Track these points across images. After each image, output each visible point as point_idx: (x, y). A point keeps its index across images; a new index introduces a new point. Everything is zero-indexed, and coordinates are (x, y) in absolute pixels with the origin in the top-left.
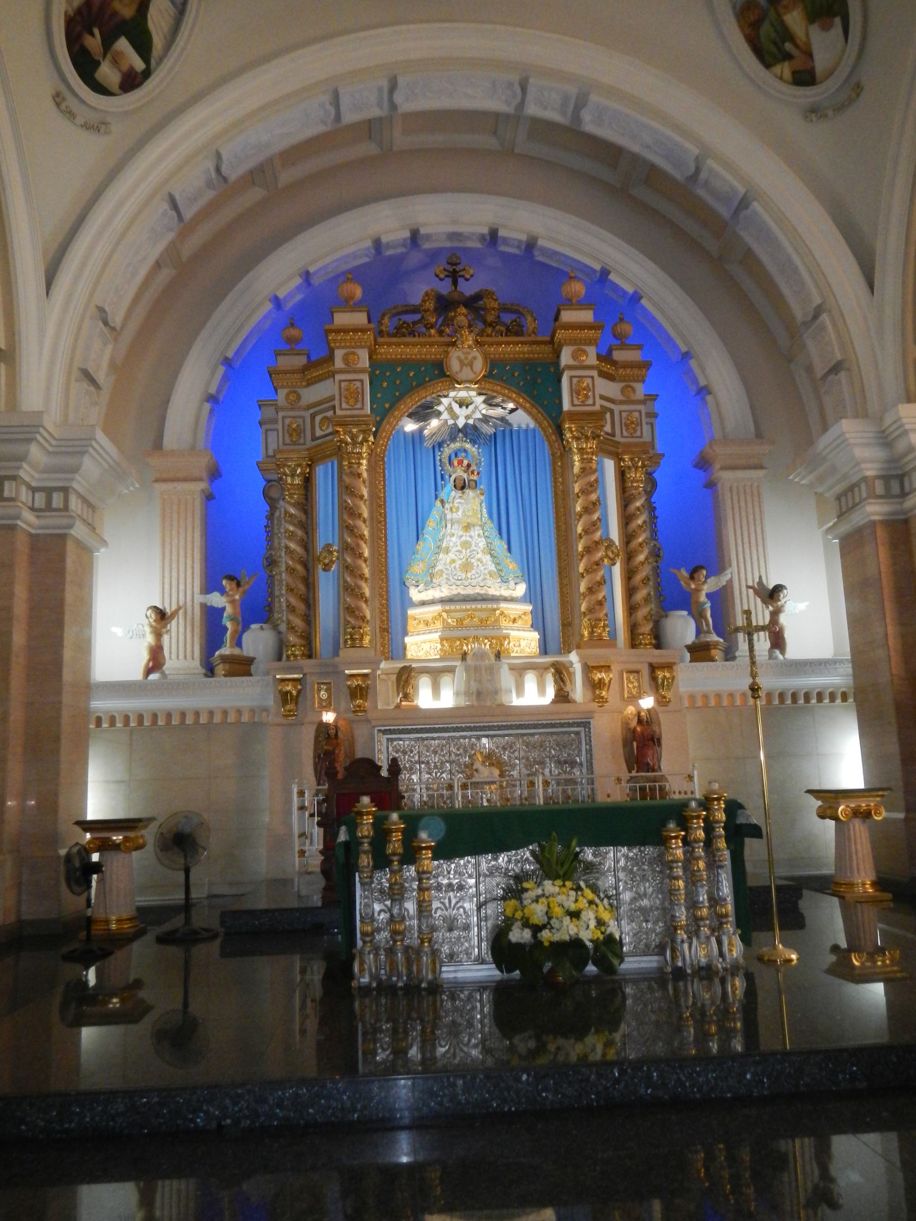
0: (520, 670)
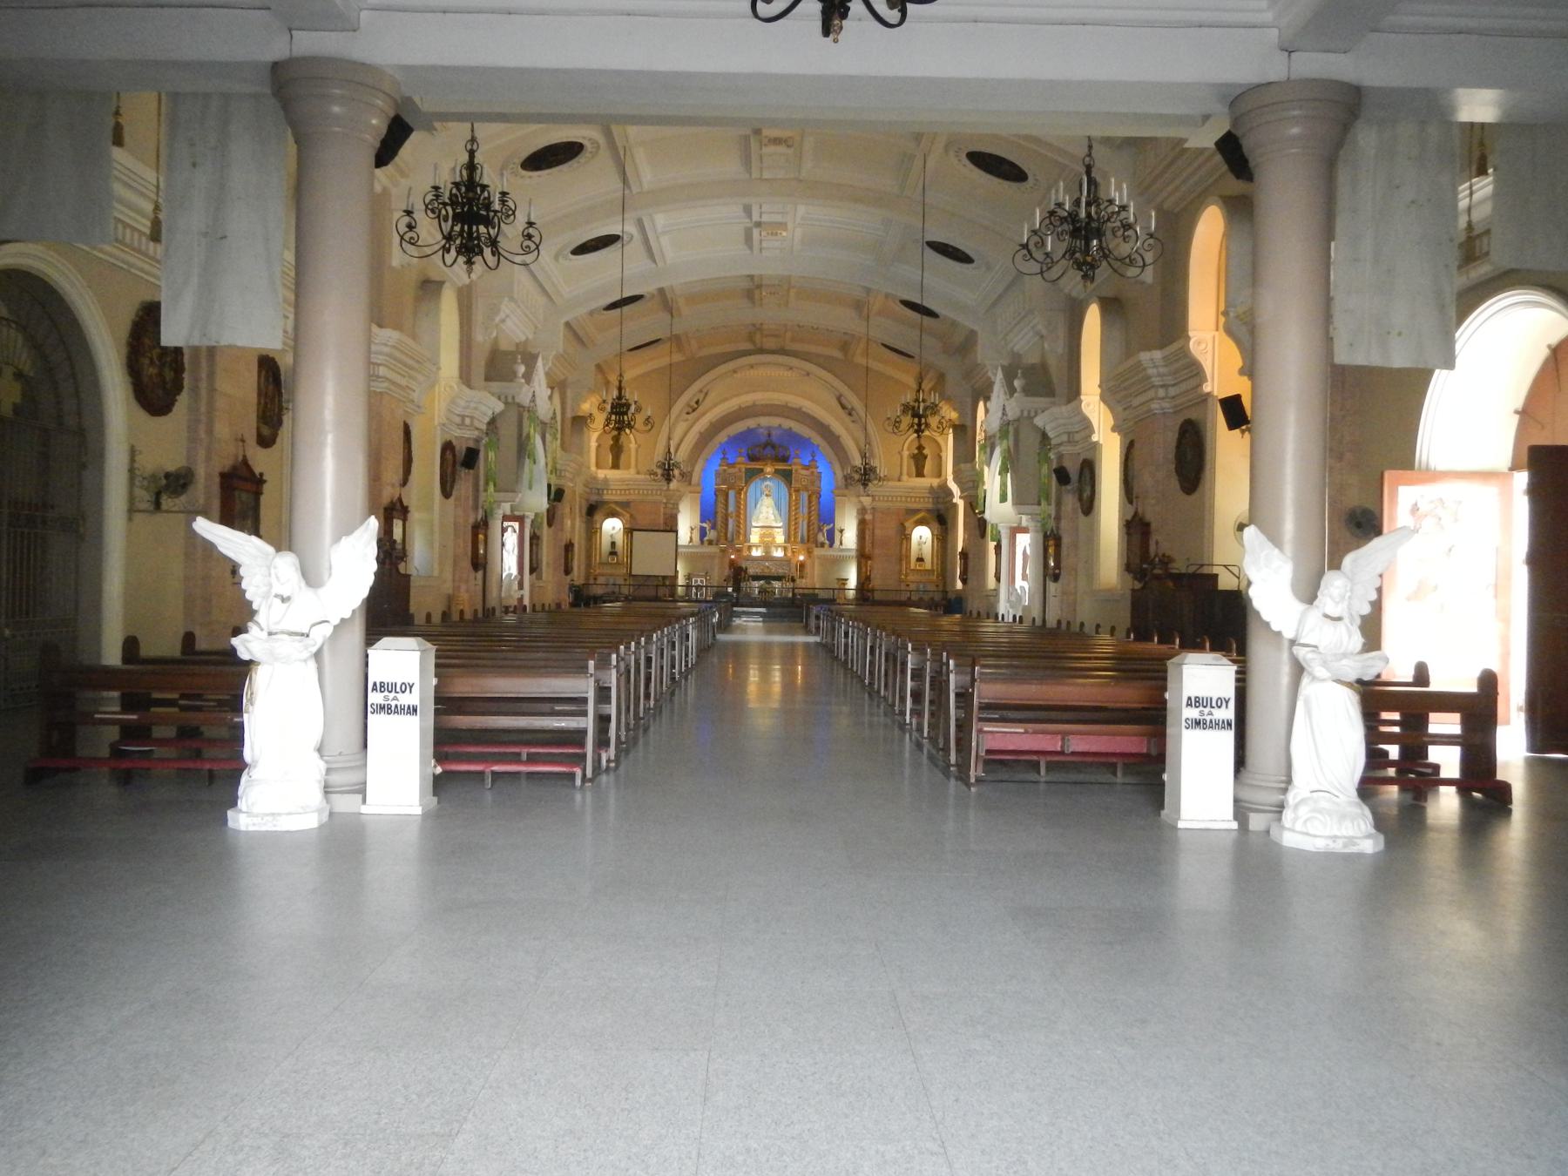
0: (777, 547)
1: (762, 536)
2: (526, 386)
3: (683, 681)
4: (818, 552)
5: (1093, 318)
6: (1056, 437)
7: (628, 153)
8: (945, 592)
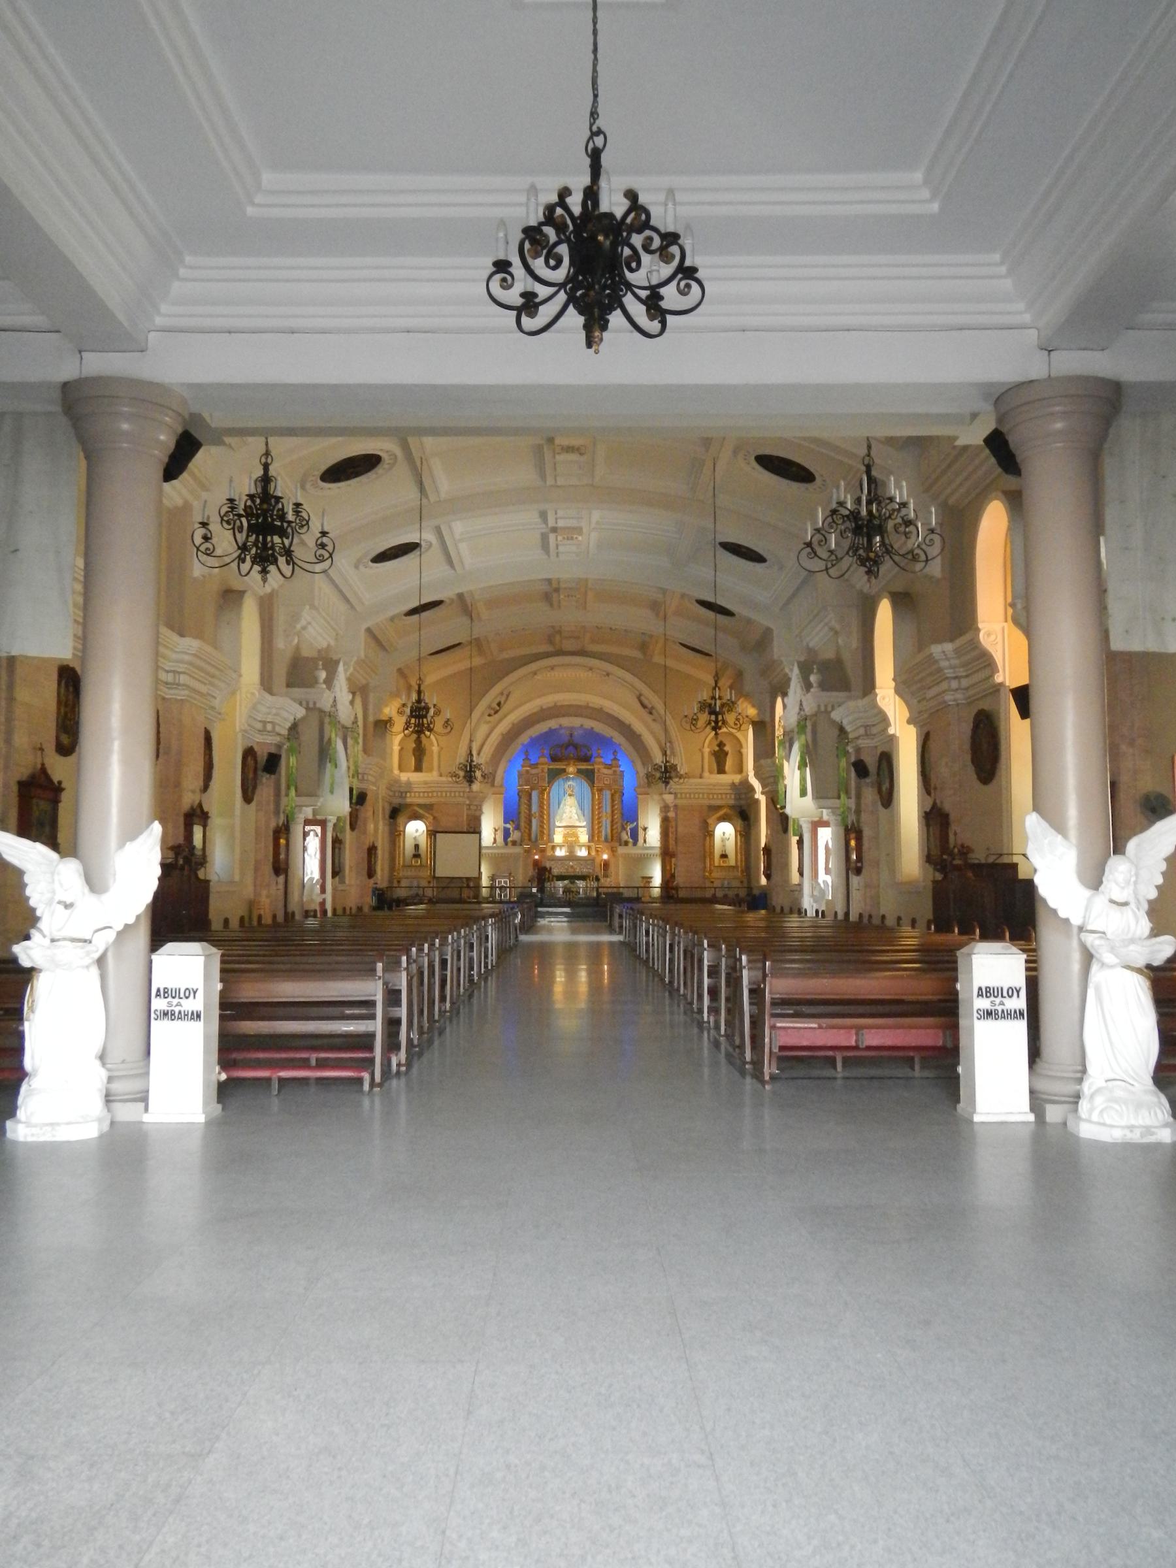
0: (581, 846)
1: (565, 836)
2: (327, 691)
3: (483, 983)
4: (621, 850)
5: (884, 612)
6: (854, 730)
7: (424, 462)
8: (750, 888)
